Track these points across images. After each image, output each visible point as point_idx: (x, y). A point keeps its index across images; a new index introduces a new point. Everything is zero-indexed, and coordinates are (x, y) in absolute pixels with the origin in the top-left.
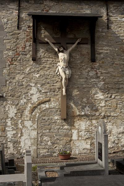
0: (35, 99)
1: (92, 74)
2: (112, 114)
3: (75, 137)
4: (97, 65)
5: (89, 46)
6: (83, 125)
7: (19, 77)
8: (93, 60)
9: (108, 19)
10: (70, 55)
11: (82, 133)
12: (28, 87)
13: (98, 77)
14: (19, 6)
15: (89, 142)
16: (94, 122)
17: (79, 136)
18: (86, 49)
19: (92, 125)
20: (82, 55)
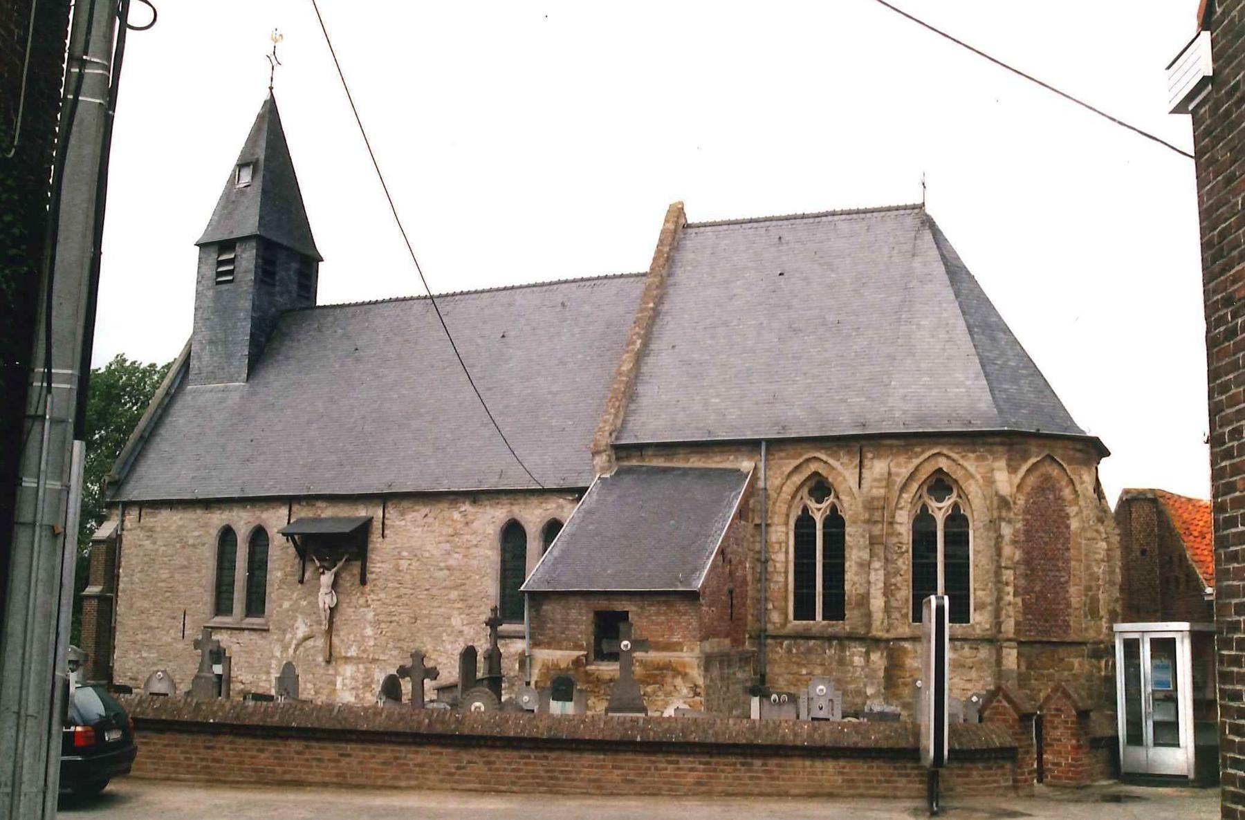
0: (300, 634)
1: (362, 601)
2: (382, 657)
3: (339, 686)
4: (368, 588)
5: (359, 563)
6: (348, 670)
7: (286, 605)
8: (363, 582)
9: (383, 523)
10: (337, 575)
11: (348, 682)
12: (294, 619)
13: (368, 606)
14: (290, 511)
15: (354, 692)
16: (361, 666)
17: (344, 685)
18: (356, 568)
19: (358, 671)
20: (353, 576)
